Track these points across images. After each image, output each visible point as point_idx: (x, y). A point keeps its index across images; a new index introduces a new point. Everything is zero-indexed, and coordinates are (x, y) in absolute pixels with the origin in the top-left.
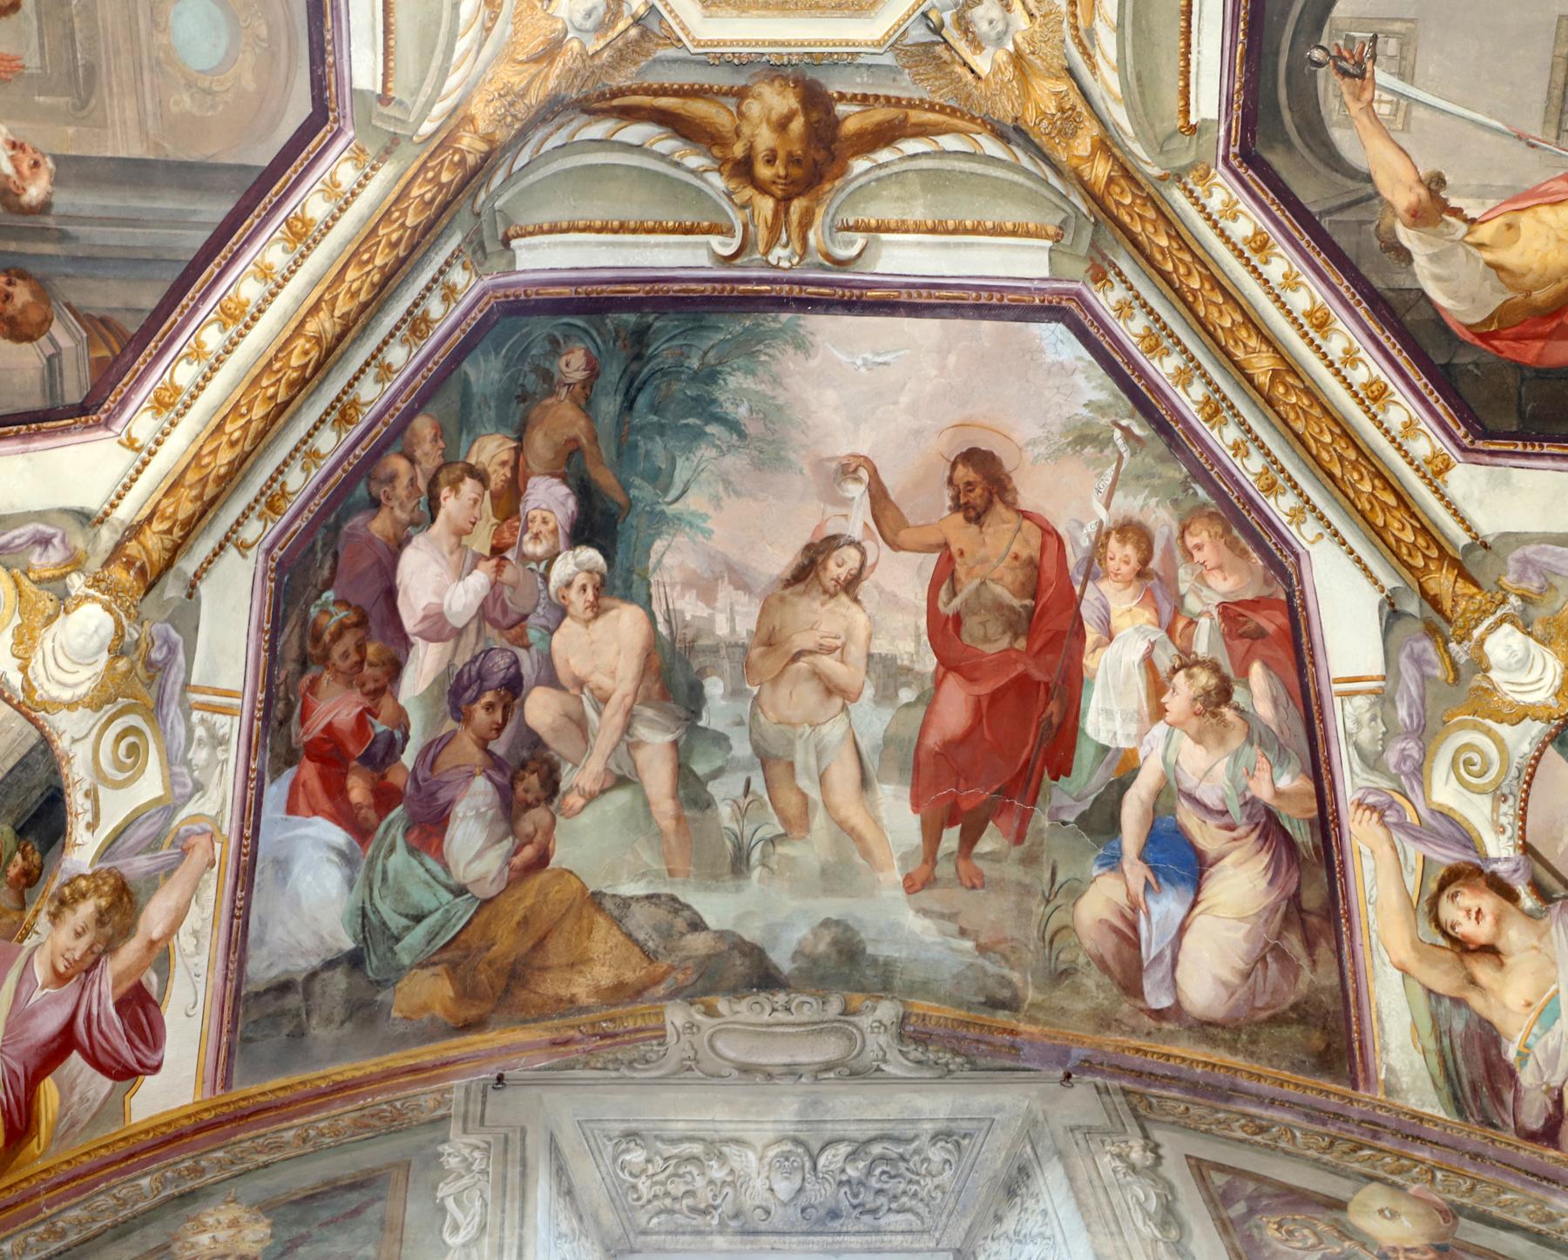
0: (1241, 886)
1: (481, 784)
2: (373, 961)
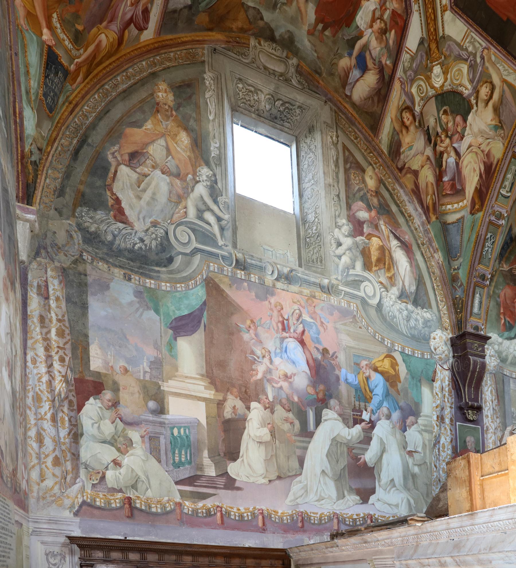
0: (371, 79)
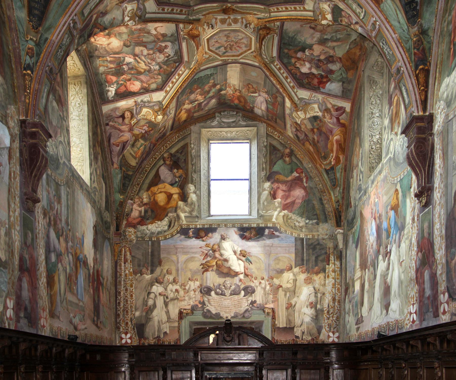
1: (329, 65)
2: (344, 80)
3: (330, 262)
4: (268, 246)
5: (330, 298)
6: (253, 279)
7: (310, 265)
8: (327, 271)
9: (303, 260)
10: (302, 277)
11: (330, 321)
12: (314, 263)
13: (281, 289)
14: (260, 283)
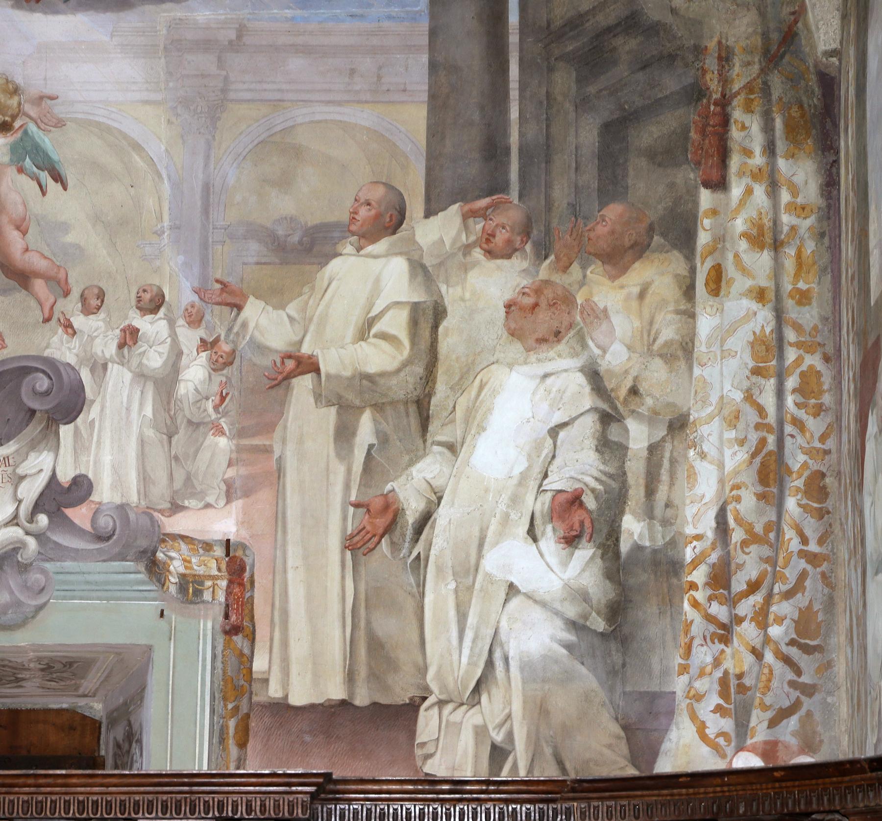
3: (735, 162)
4: (205, 45)
5: (735, 458)
6: (71, 306)
7: (561, 194)
8: (703, 238)
9: (494, 150)
10: (493, 284)
11: (737, 658)
12: (590, 177)
13: (304, 384)
14: (130, 337)
